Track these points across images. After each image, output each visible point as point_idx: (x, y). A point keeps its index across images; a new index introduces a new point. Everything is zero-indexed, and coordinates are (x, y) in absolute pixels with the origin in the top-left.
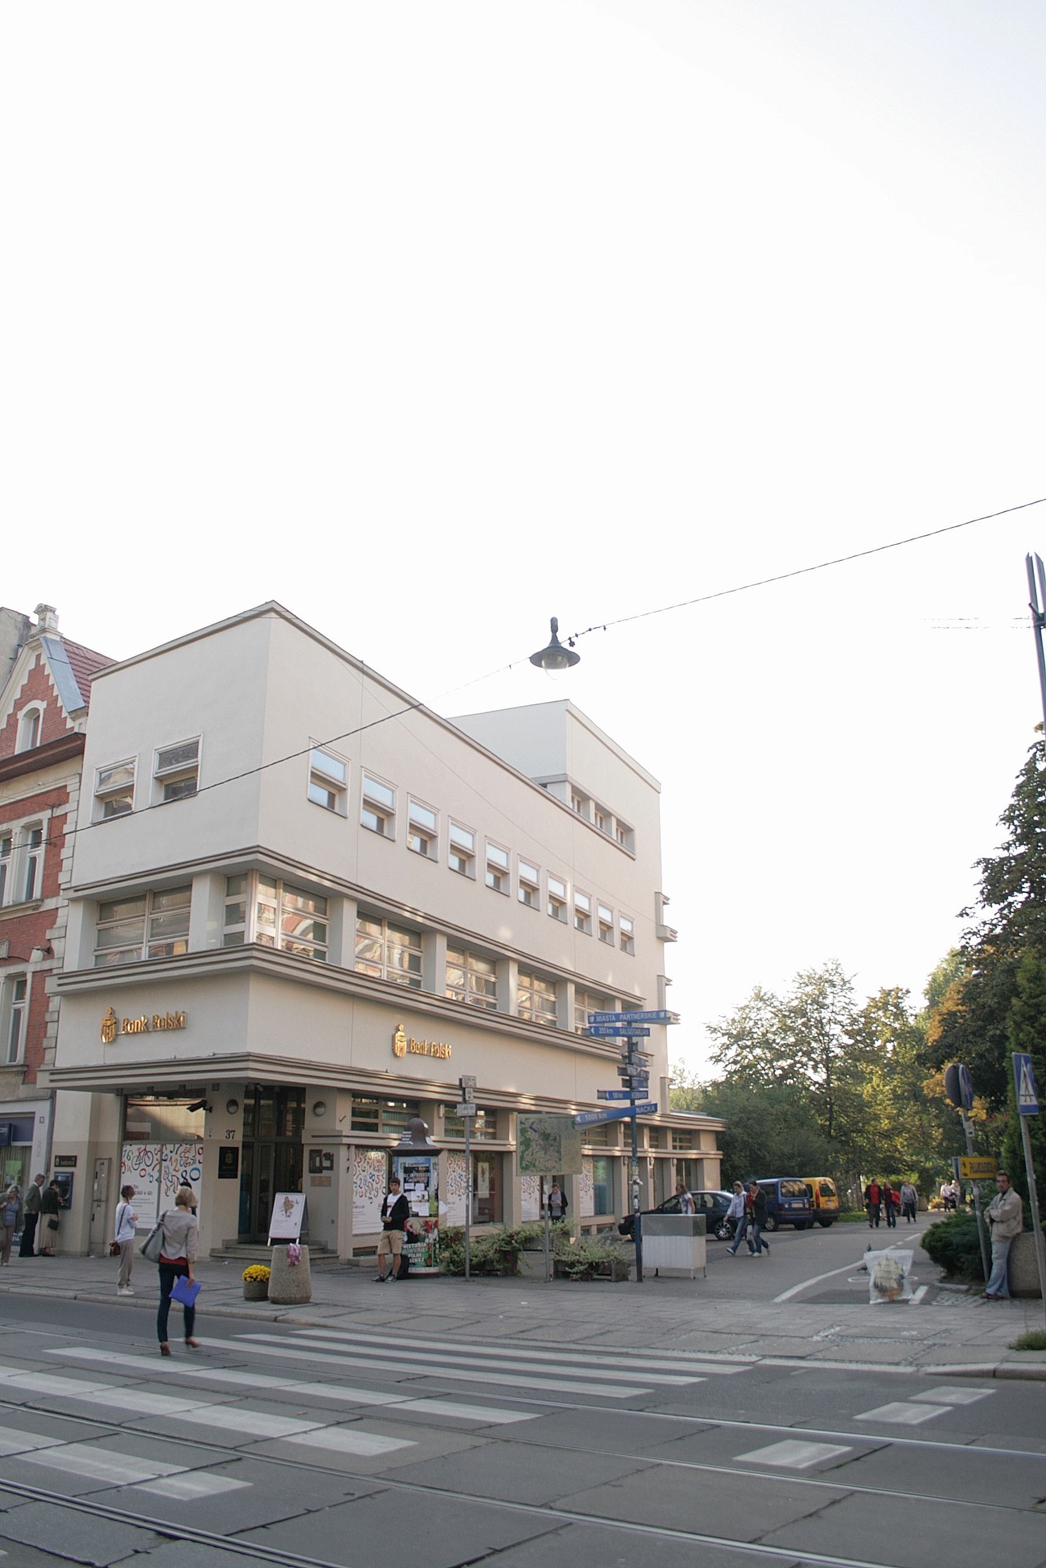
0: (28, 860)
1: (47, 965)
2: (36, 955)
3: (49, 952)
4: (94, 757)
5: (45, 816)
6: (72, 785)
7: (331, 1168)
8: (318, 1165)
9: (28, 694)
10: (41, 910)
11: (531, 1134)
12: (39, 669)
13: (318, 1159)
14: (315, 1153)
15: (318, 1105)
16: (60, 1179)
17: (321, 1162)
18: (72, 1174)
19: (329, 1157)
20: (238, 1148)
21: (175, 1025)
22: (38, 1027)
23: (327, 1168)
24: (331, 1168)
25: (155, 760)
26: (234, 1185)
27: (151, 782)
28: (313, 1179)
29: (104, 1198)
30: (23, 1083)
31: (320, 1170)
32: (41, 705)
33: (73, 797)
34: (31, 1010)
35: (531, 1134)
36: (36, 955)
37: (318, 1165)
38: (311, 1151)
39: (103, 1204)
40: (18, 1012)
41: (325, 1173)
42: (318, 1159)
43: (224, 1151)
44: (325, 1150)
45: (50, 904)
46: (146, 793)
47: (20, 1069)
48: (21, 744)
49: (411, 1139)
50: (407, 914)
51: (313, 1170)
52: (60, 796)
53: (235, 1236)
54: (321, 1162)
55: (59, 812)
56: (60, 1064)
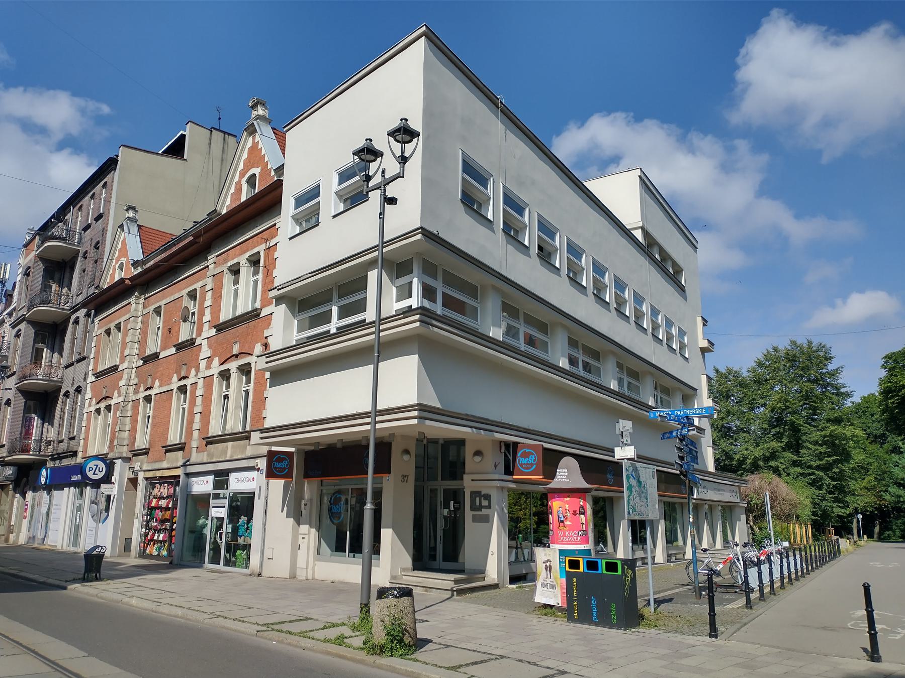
0: (252, 283)
5: (261, 248)
7: (489, 507)
8: (478, 504)
9: (249, 165)
13: (478, 499)
14: (475, 494)
19: (488, 497)
22: (261, 402)
23: (486, 507)
24: (489, 507)
25: (336, 177)
27: (334, 196)
28: (474, 516)
31: (480, 508)
32: (256, 171)
34: (255, 390)
37: (478, 504)
40: (247, 392)
41: (484, 511)
42: (478, 499)
56: (268, 424)
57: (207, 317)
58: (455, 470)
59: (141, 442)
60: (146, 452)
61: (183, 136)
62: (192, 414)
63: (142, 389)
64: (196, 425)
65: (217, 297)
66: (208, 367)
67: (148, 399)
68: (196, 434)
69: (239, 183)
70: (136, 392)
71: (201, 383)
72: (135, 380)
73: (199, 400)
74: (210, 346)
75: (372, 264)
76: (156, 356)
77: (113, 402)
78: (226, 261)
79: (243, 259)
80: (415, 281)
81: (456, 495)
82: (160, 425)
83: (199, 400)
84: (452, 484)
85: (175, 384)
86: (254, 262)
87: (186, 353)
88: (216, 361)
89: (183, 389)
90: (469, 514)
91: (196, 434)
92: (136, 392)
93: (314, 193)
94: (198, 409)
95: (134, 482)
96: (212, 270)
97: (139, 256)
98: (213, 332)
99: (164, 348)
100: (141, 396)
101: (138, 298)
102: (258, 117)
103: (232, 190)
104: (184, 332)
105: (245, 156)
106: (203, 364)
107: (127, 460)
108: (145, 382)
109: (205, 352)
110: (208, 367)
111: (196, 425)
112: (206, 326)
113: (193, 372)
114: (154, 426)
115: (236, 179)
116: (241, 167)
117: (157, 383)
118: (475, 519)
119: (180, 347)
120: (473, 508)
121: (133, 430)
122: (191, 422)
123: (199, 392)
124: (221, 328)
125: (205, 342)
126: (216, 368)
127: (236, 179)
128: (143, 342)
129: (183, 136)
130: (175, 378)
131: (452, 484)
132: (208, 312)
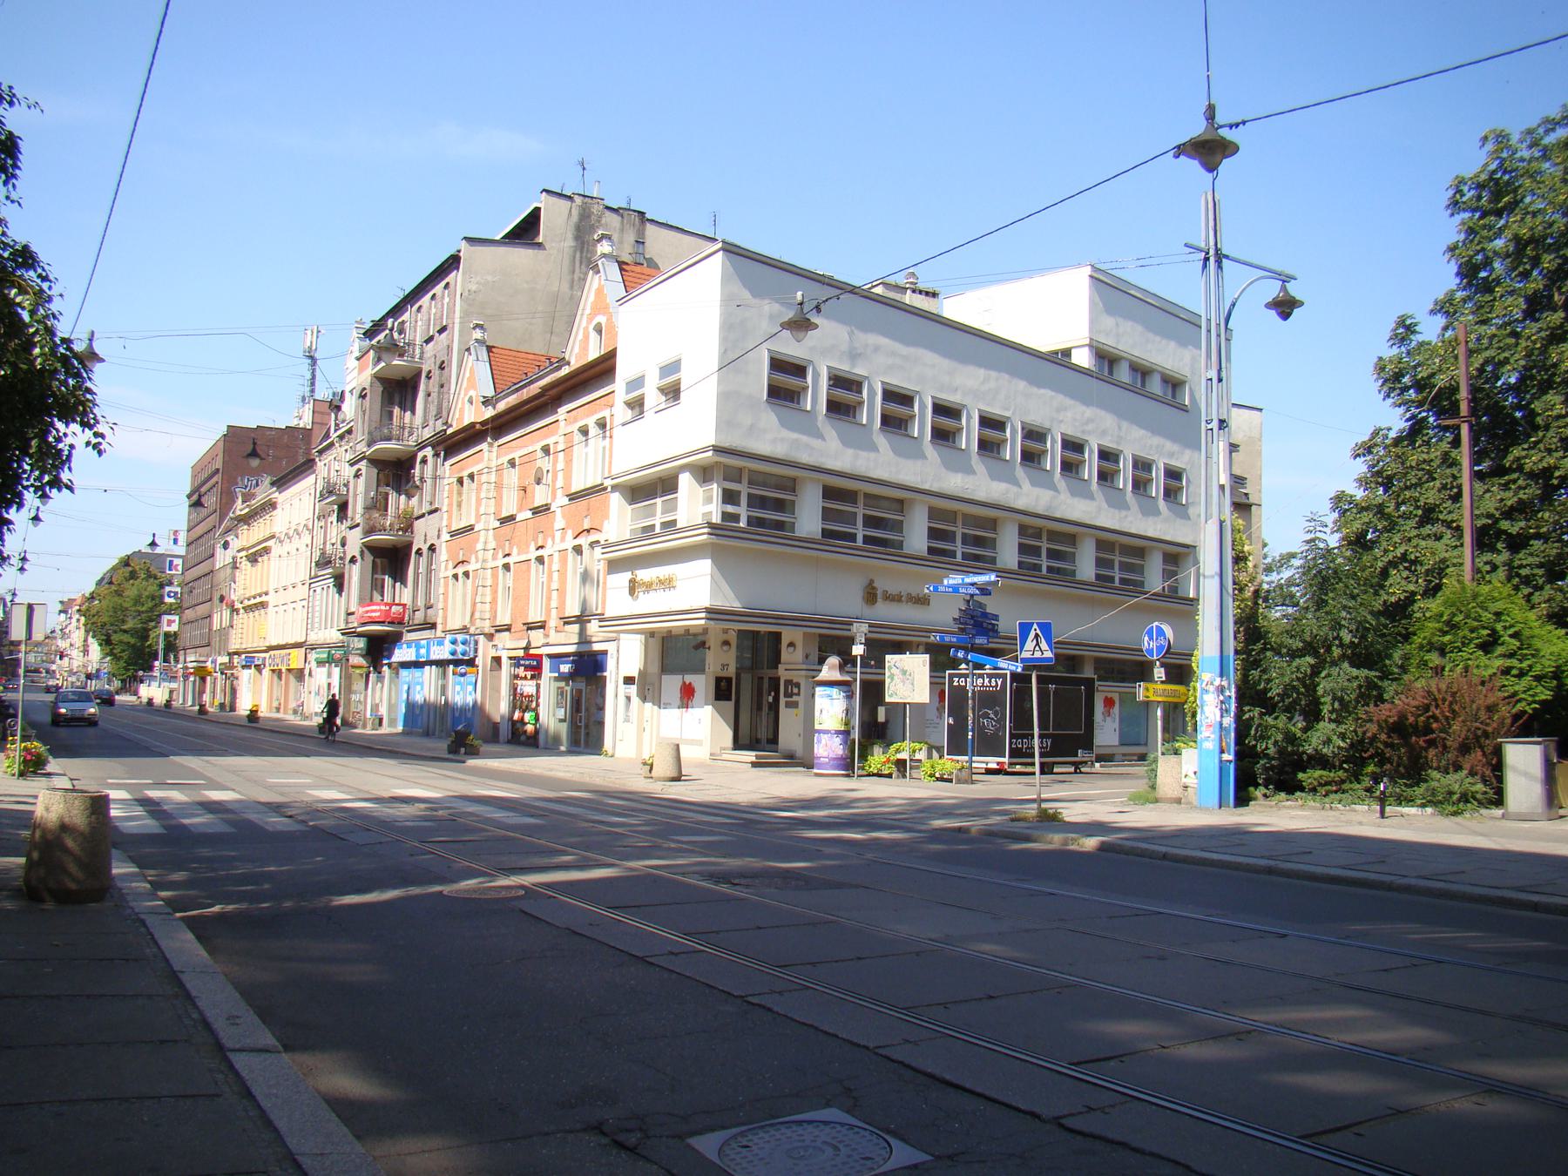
4: (624, 370)
11: (894, 670)
12: (600, 291)
14: (789, 682)
19: (798, 685)
21: (667, 584)
32: (602, 319)
35: (894, 670)
41: (795, 698)
43: (718, 680)
46: (653, 398)
48: (593, 354)
57: (560, 483)
58: (776, 660)
59: (504, 619)
60: (508, 628)
61: (537, 210)
62: (550, 591)
63: (500, 555)
64: (554, 604)
65: (569, 462)
66: (563, 539)
67: (507, 567)
68: (554, 612)
69: (586, 329)
70: (494, 558)
71: (556, 555)
72: (492, 545)
73: (556, 575)
74: (564, 516)
75: (683, 468)
76: (512, 518)
77: (470, 568)
78: (575, 420)
79: (591, 422)
80: (715, 486)
81: (775, 682)
82: (520, 598)
83: (556, 575)
84: (771, 673)
85: (533, 554)
86: (602, 425)
87: (541, 518)
88: (570, 534)
89: (540, 560)
90: (783, 700)
91: (554, 612)
92: (494, 558)
93: (637, 383)
94: (555, 586)
95: (497, 660)
96: (563, 428)
97: (490, 393)
98: (566, 501)
99: (521, 509)
100: (501, 562)
101: (491, 445)
102: (604, 255)
103: (580, 336)
104: (540, 496)
105: (592, 298)
106: (558, 535)
107: (490, 637)
108: (503, 547)
109: (559, 522)
110: (563, 539)
111: (554, 604)
112: (559, 493)
113: (550, 541)
114: (515, 599)
115: (584, 324)
116: (588, 311)
117: (515, 551)
118: (788, 705)
119: (536, 511)
121: (494, 602)
122: (549, 599)
123: (555, 567)
124: (573, 497)
125: (559, 511)
126: (570, 543)
127: (584, 324)
128: (498, 499)
129: (537, 210)
130: (532, 547)
131: (771, 673)
132: (560, 475)
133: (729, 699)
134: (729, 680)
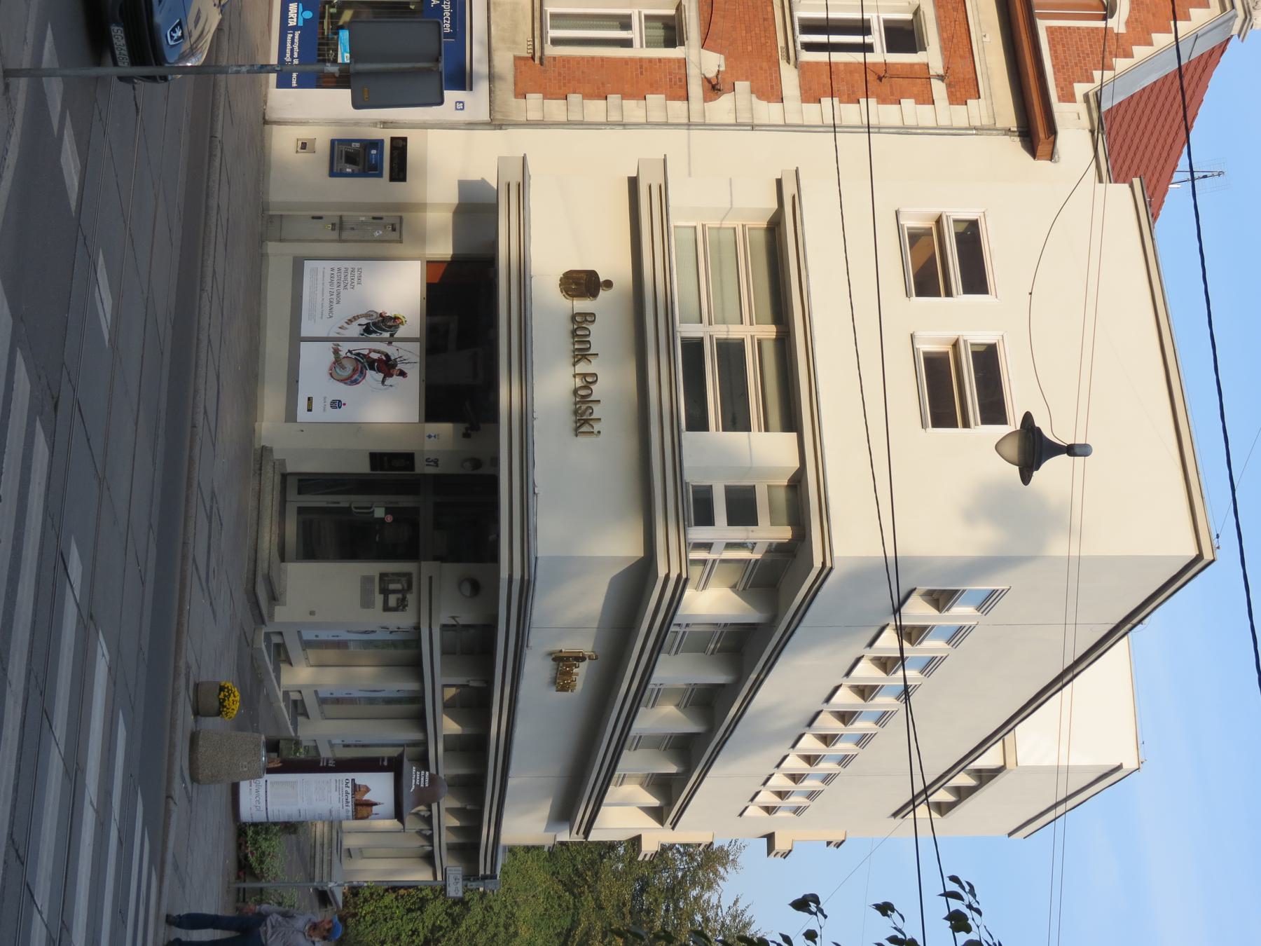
1: (696, 89)
2: (712, 63)
3: (714, 88)
5: (932, 56)
6: (976, 111)
7: (386, 608)
10: (783, 64)
13: (398, 586)
15: (476, 587)
16: (374, 152)
17: (394, 592)
18: (380, 175)
19: (402, 605)
20: (413, 469)
23: (386, 601)
24: (386, 608)
26: (363, 467)
29: (345, 235)
30: (517, 59)
31: (385, 592)
33: (960, 115)
34: (626, 61)
36: (712, 63)
38: (408, 575)
39: (335, 235)
41: (379, 599)
42: (398, 586)
44: (411, 598)
45: (789, 78)
47: (538, 55)
49: (418, 787)
50: (753, 676)
51: (382, 576)
52: (963, 86)
53: (290, 468)
54: (394, 592)
55: (939, 89)
90: (373, 569)
118: (367, 580)
120: (382, 576)
133: (373, 468)
134: (412, 468)
